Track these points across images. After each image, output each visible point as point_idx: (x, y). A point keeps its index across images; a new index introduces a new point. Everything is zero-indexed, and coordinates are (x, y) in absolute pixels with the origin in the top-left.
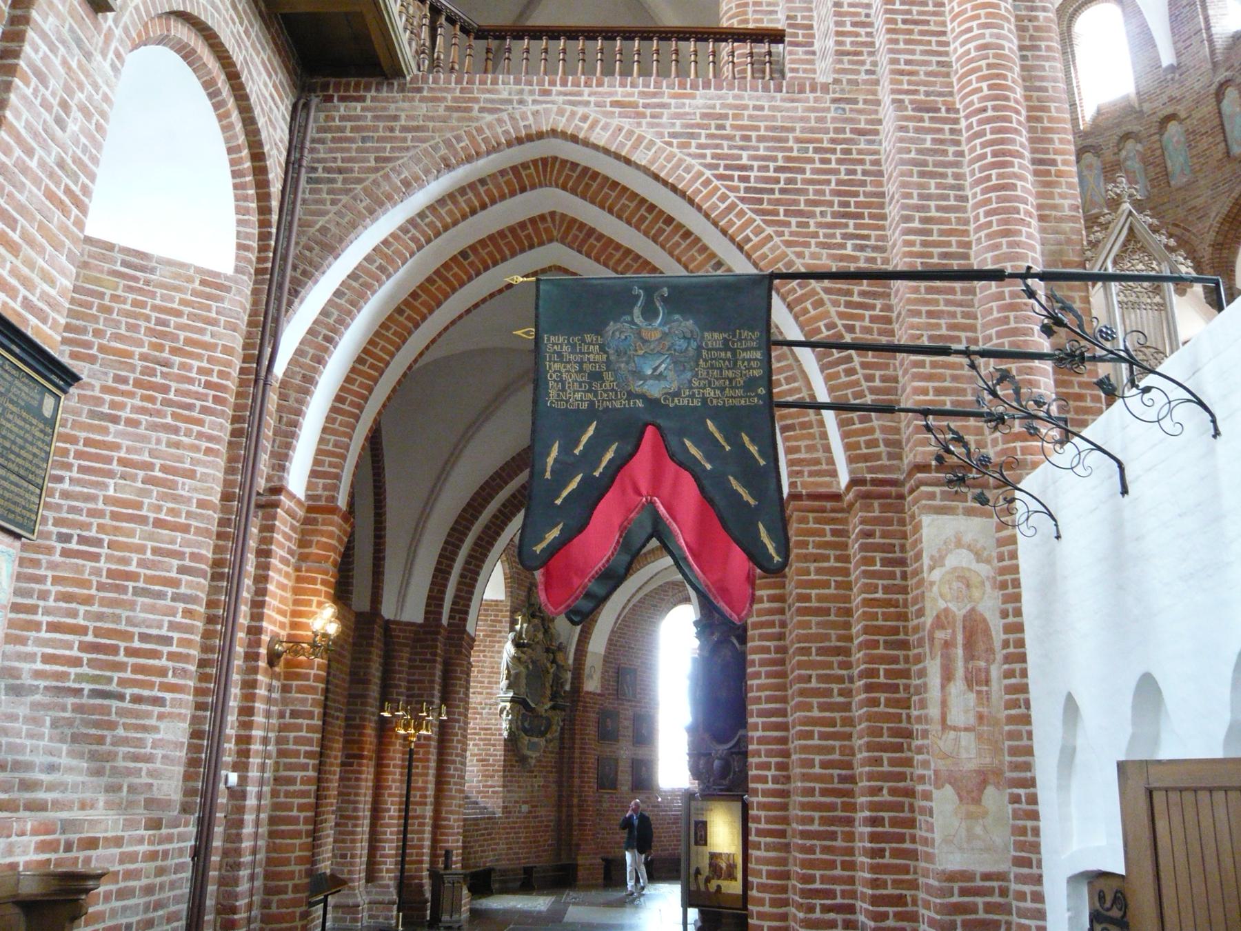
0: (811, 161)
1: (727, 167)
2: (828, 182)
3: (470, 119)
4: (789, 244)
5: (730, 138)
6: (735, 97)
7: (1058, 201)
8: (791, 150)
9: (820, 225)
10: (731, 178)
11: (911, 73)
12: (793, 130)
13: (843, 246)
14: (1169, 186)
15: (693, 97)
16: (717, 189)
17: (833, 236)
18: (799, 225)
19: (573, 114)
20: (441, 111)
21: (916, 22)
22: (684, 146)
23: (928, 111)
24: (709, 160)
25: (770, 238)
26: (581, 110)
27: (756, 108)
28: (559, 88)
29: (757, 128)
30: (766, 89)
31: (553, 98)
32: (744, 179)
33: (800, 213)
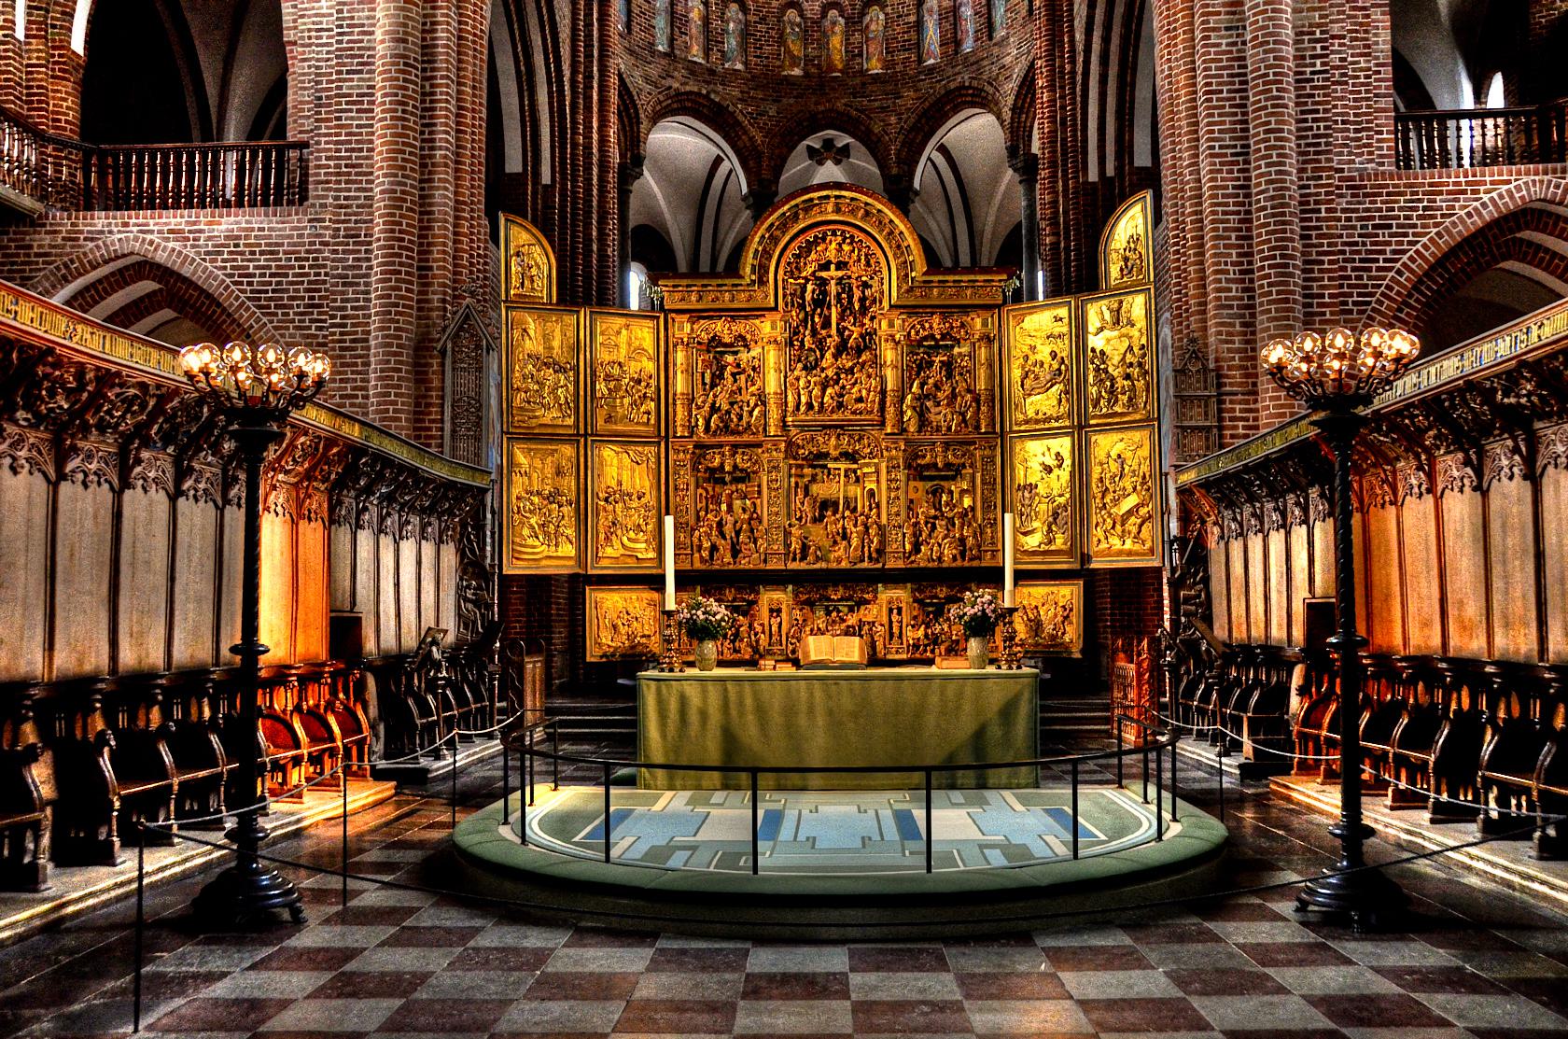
0: (292, 267)
1: (240, 276)
2: (302, 283)
3: (80, 246)
4: (276, 328)
5: (242, 253)
6: (247, 222)
7: (431, 296)
8: (280, 260)
9: (295, 314)
10: (242, 283)
11: (347, 207)
12: (282, 245)
13: (310, 328)
14: (990, 38)
15: (220, 224)
16: (233, 291)
17: (304, 321)
18: (283, 314)
19: (144, 240)
20: (60, 241)
21: (353, 166)
22: (213, 261)
23: (352, 236)
24: (229, 271)
25: (265, 324)
26: (149, 237)
27: (260, 229)
28: (134, 221)
29: (260, 245)
30: (266, 215)
31: (131, 228)
32: (250, 284)
33: (285, 306)
